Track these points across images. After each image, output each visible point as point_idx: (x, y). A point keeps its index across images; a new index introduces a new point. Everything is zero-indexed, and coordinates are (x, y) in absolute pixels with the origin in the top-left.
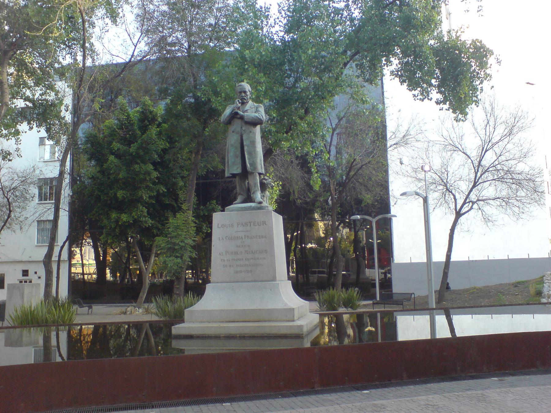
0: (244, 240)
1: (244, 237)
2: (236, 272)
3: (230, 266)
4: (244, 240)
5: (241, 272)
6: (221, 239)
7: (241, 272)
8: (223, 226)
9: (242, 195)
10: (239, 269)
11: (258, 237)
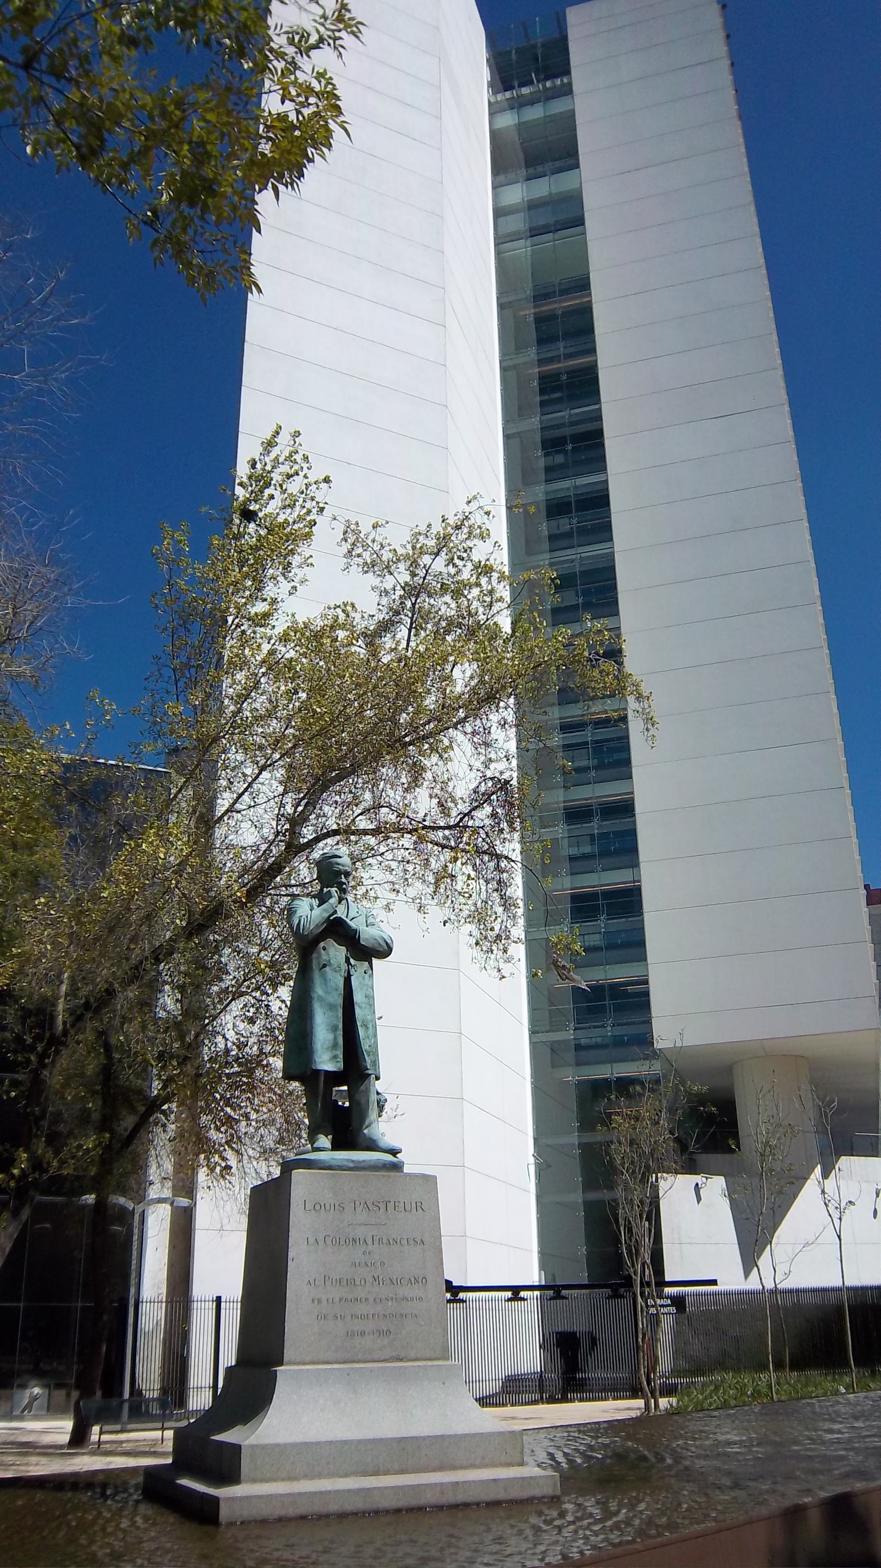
0: (370, 1247)
1: (370, 1242)
2: (351, 1334)
5: (363, 1334)
6: (312, 1240)
8: (318, 1207)
10: (357, 1326)
11: (404, 1242)
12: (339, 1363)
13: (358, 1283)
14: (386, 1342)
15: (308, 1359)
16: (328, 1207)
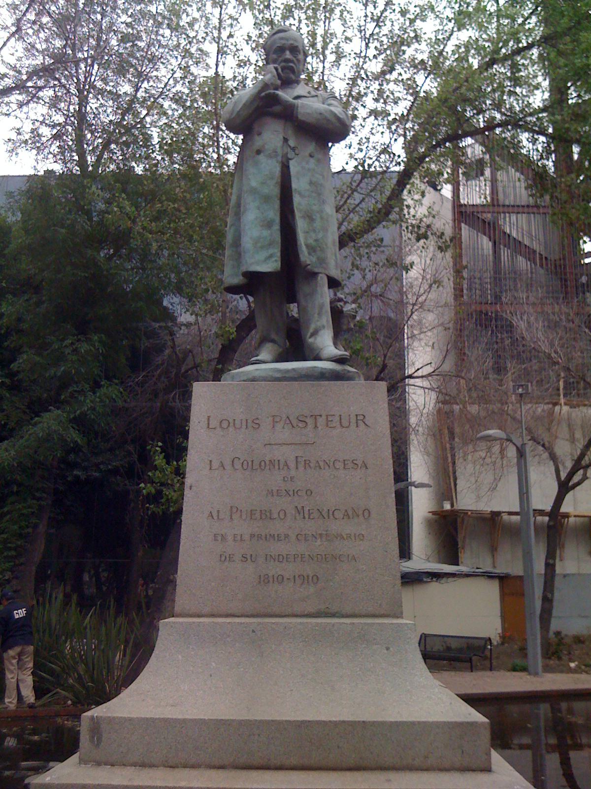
1: (292, 465)
2: (264, 580)
3: (244, 558)
4: (293, 472)
5: (280, 579)
6: (216, 464)
7: (280, 579)
8: (225, 424)
9: (273, 341)
10: (274, 569)
11: (339, 465)
12: (248, 616)
13: (275, 516)
14: (312, 589)
15: (207, 610)
16: (238, 422)
